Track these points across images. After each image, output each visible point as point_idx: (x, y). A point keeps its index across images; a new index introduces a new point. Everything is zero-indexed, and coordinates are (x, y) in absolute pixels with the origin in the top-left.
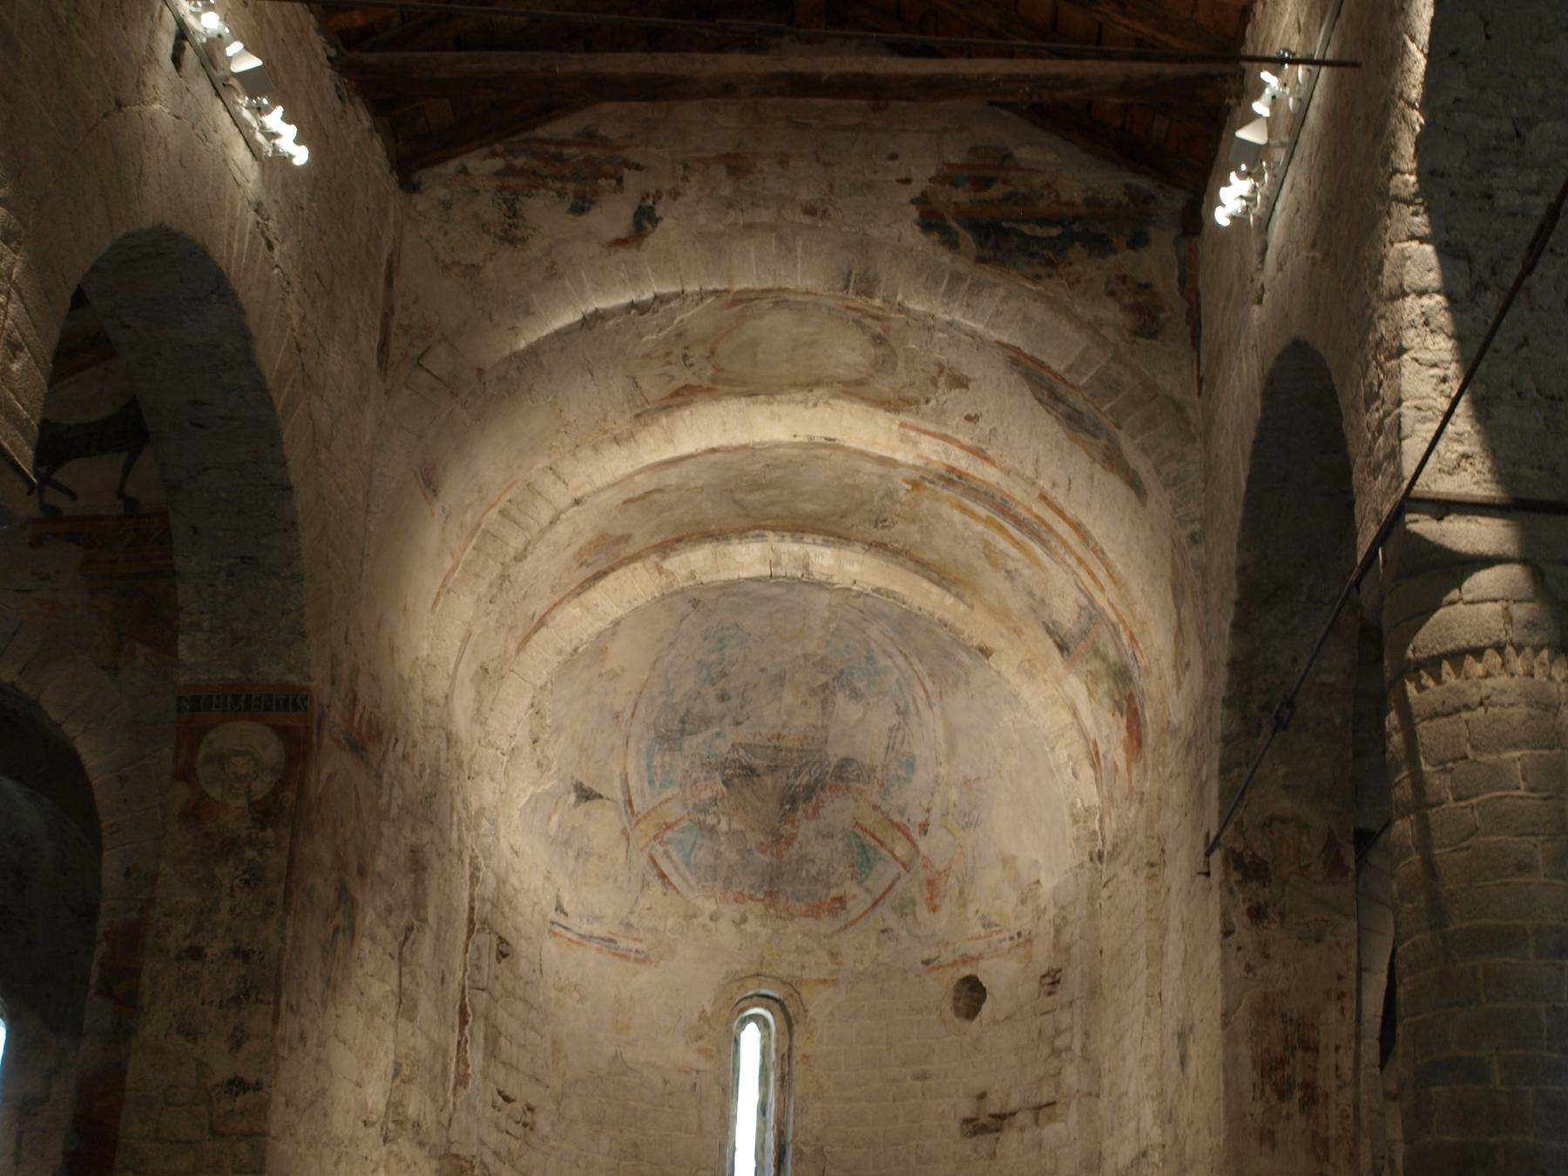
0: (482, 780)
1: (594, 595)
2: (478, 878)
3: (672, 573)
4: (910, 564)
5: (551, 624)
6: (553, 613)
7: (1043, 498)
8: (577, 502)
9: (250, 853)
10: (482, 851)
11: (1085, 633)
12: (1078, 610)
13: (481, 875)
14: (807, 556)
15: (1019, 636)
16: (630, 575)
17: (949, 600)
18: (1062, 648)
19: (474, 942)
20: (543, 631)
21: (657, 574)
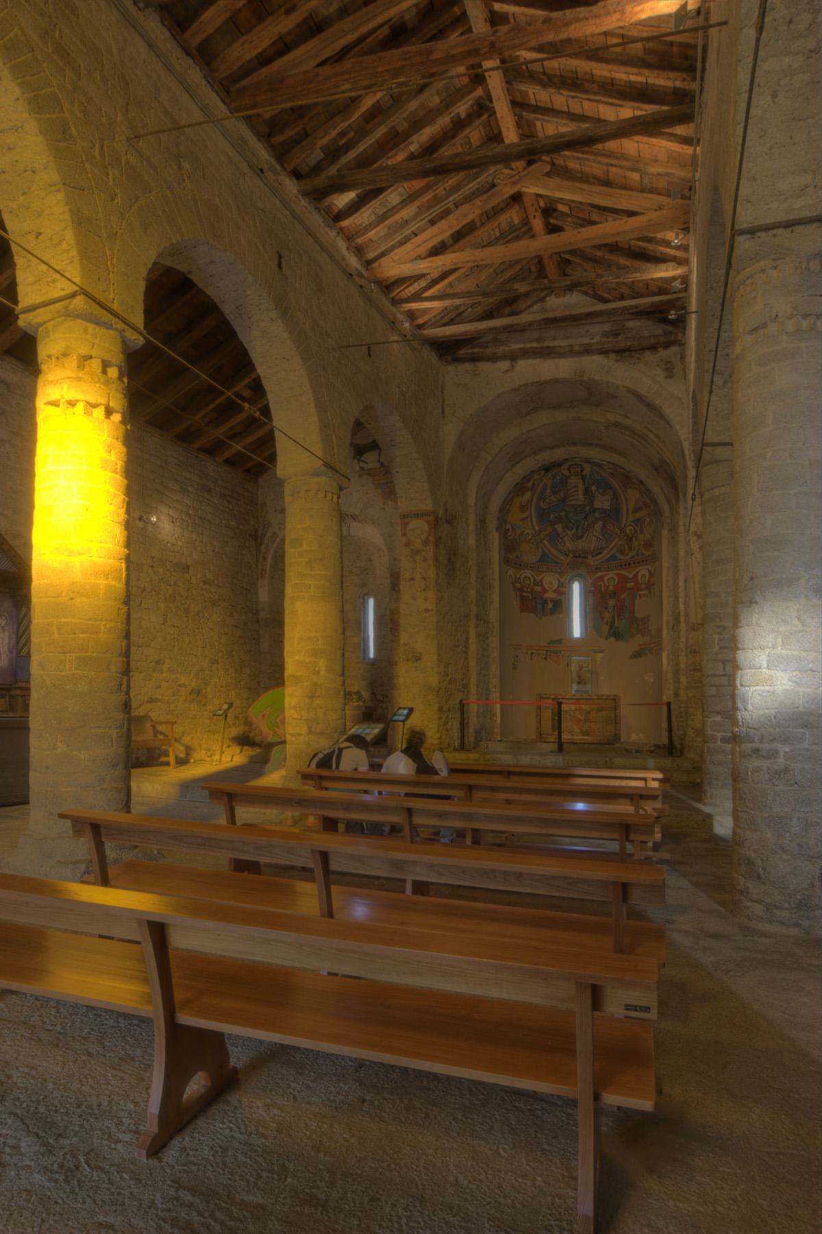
7: (646, 428)
8: (506, 445)
9: (423, 553)
18: (656, 470)
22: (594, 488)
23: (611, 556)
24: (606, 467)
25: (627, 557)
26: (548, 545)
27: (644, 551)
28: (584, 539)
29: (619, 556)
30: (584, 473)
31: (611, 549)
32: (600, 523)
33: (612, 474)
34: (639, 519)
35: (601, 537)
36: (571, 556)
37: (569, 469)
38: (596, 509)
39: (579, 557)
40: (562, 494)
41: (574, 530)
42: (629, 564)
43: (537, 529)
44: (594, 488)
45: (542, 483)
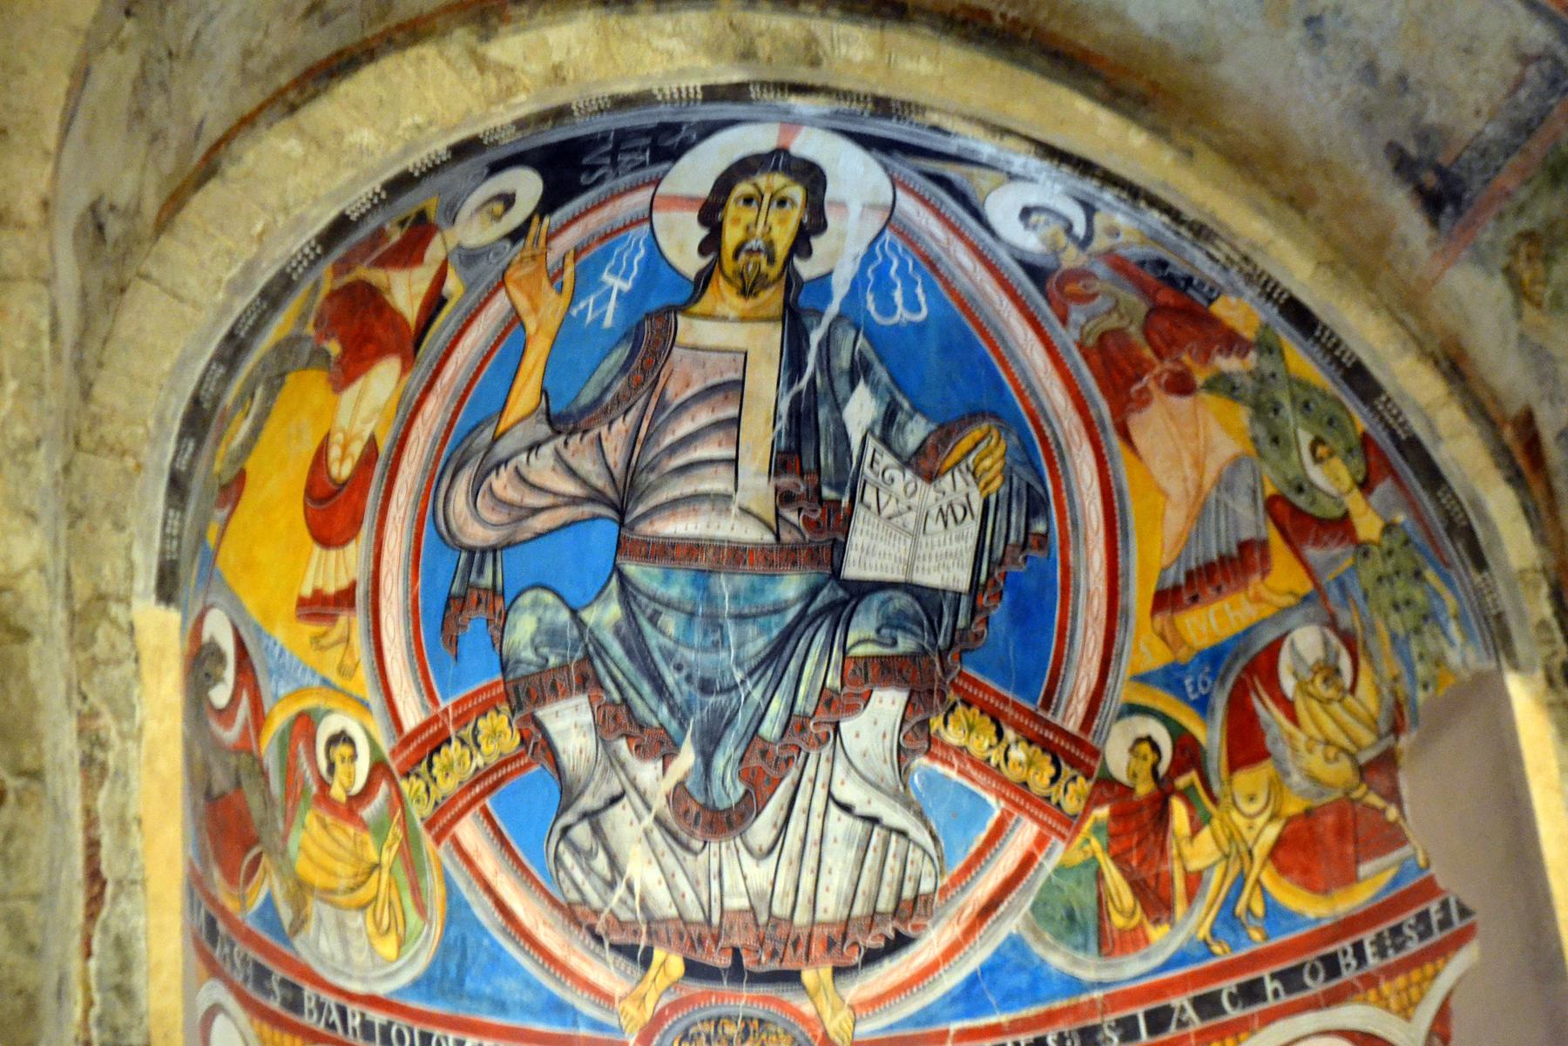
0: (93, 530)
1: (328, 111)
2: (103, 768)
3: (511, 70)
4: (1042, 62)
5: (231, 171)
6: (236, 146)
10: (109, 700)
11: (1525, 129)
12: (1515, 69)
13: (111, 759)
14: (811, 41)
15: (1302, 211)
16: (410, 71)
17: (1138, 139)
19: (105, 929)
20: (213, 186)
21: (473, 71)
22: (861, 410)
23: (989, 970)
24: (1002, 207)
25: (1131, 968)
26: (489, 862)
27: (1291, 897)
28: (762, 830)
29: (1058, 959)
30: (807, 269)
31: (989, 908)
32: (888, 703)
33: (1036, 272)
34: (1215, 657)
35: (895, 816)
36: (669, 963)
37: (711, 213)
38: (862, 590)
39: (737, 972)
40: (616, 437)
41: (687, 758)
42: (1158, 1020)
43: (412, 717)
44: (861, 410)
45: (498, 307)
